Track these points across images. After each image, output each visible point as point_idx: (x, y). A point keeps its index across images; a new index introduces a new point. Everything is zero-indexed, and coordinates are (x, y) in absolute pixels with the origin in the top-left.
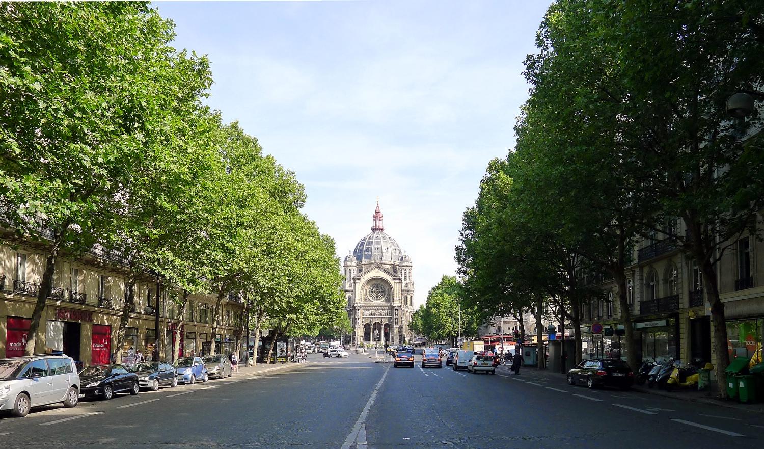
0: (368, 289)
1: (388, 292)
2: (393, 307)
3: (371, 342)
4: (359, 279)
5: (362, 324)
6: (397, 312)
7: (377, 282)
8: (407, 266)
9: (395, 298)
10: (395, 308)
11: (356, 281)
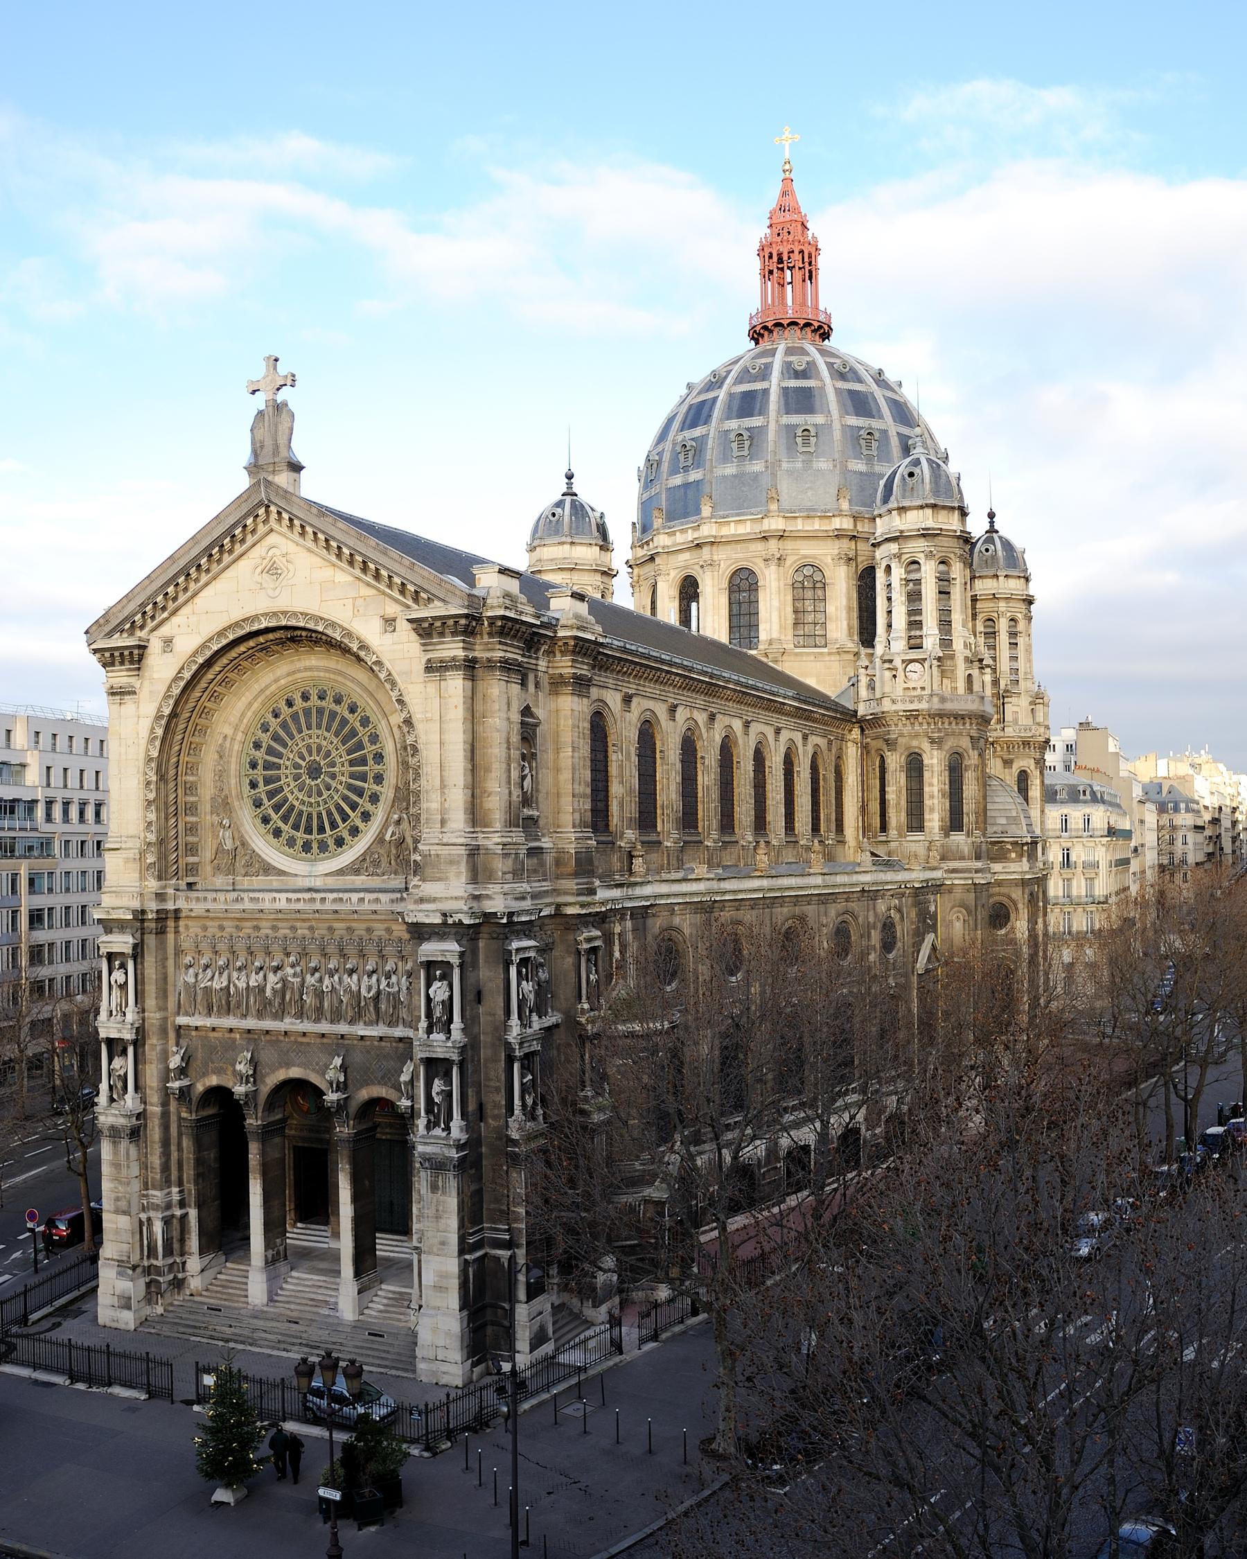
10: (431, 949)
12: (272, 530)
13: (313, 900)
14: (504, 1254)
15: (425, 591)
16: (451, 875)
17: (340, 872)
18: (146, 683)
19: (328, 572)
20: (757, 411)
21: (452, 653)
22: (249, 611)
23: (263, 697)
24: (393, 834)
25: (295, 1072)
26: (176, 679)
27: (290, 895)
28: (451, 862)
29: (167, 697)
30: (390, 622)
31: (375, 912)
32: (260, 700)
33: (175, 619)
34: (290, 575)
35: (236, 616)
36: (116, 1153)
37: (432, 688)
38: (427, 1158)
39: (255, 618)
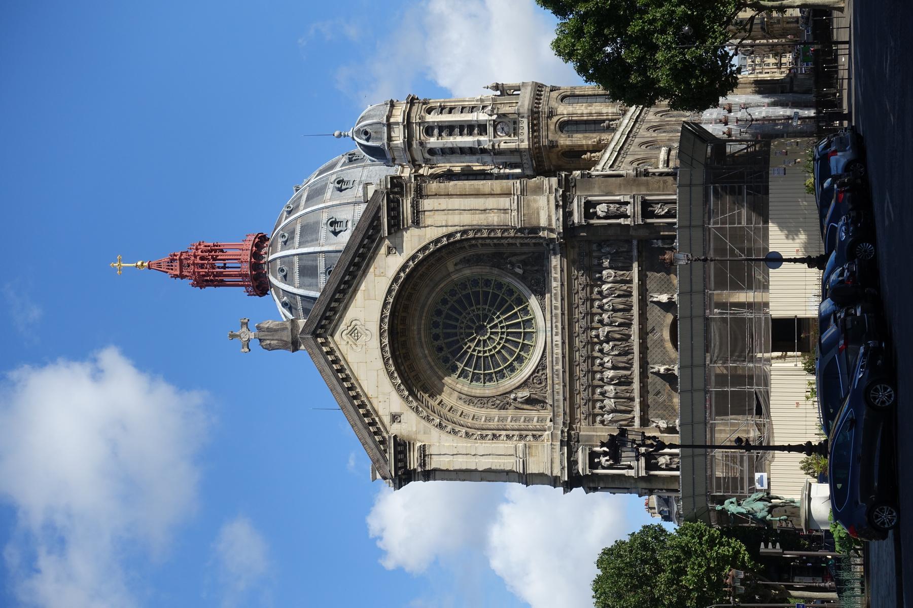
0: (464, 386)
1: (477, 260)
2: (569, 229)
6: (601, 209)
7: (418, 329)
8: (408, 125)
9: (513, 220)
10: (576, 218)
11: (414, 462)
12: (332, 335)
13: (556, 315)
15: (372, 222)
17: (543, 309)
18: (419, 437)
19: (359, 295)
20: (314, 263)
22: (377, 353)
23: (435, 367)
24: (519, 267)
28: (528, 206)
31: (562, 271)
32: (437, 370)
33: (380, 413)
34: (358, 323)
35: (380, 364)
37: (428, 219)
39: (382, 349)
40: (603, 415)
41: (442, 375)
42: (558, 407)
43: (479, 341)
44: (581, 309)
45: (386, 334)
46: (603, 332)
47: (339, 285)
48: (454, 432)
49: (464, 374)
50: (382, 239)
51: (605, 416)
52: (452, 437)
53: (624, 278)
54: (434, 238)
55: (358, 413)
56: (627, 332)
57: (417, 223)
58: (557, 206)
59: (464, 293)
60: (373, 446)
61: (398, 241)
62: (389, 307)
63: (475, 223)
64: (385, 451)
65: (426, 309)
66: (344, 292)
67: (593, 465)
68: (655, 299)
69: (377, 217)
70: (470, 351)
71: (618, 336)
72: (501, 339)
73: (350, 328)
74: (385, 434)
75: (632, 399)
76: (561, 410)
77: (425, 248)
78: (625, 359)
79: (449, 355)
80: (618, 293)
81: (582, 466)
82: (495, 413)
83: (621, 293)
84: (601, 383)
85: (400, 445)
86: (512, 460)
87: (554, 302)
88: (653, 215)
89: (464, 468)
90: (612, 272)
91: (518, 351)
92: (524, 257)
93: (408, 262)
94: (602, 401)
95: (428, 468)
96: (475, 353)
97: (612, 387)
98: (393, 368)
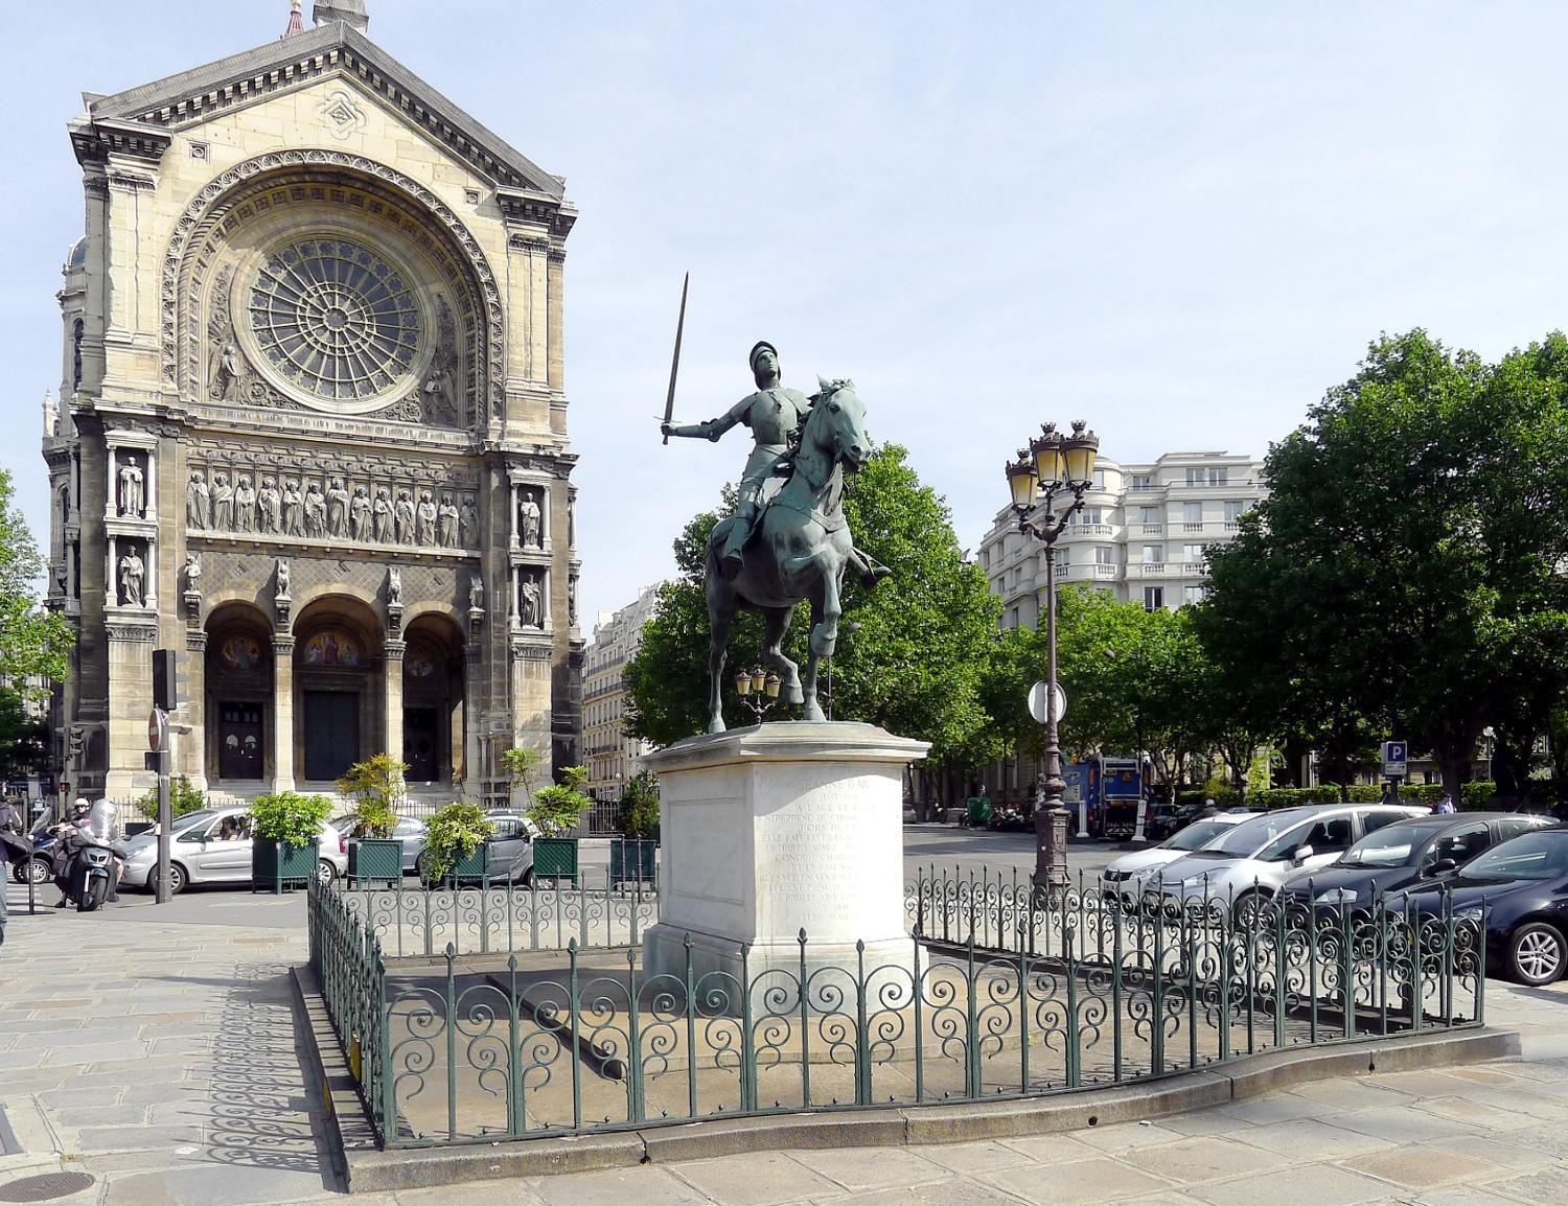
1: (447, 330)
2: (501, 460)
3: (284, 780)
4: (151, 149)
5: (188, 609)
6: (530, 507)
10: (520, 474)
11: (118, 163)
12: (341, 77)
14: (569, 736)
15: (518, 175)
16: (536, 417)
19: (406, 134)
21: (540, 235)
22: (311, 142)
25: (337, 588)
26: (212, 187)
27: (340, 422)
28: (536, 407)
29: (197, 203)
30: (472, 194)
31: (437, 446)
34: (361, 122)
36: (131, 655)
37: (519, 258)
38: (522, 648)
39: (317, 152)
40: (206, 481)
41: (265, 246)
42: (220, 414)
43: (321, 313)
44: (377, 467)
45: (341, 163)
46: (341, 494)
47: (423, 104)
48: (176, 241)
49: (267, 279)
50: (492, 186)
51: (204, 485)
52: (168, 235)
53: (425, 534)
54: (492, 264)
55: (211, 87)
56: (341, 530)
57: (515, 241)
58: (538, 447)
59: (396, 301)
60: (153, 100)
61: (488, 210)
62: (385, 176)
63: (512, 327)
64: (144, 120)
65: (372, 240)
66: (411, 110)
67: (123, 453)
68: (393, 576)
69: (524, 183)
70: (304, 295)
71: (335, 516)
72: (324, 346)
73: (352, 108)
74: (172, 126)
75: (233, 527)
76: (213, 418)
77: (476, 248)
78: (299, 522)
79: (297, 262)
80: (403, 523)
81: (117, 436)
82: (204, 317)
83: (402, 528)
84: (259, 485)
85: (154, 146)
86: (130, 327)
87: (390, 428)
88: (523, 580)
89: (113, 245)
90: (434, 517)
91: (304, 367)
92: (450, 396)
93: (455, 217)
94: (229, 483)
95: (111, 185)
96: (300, 303)
97: (253, 500)
98: (285, 163)
